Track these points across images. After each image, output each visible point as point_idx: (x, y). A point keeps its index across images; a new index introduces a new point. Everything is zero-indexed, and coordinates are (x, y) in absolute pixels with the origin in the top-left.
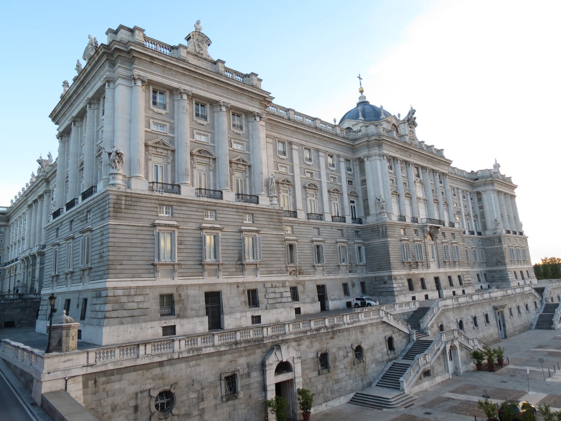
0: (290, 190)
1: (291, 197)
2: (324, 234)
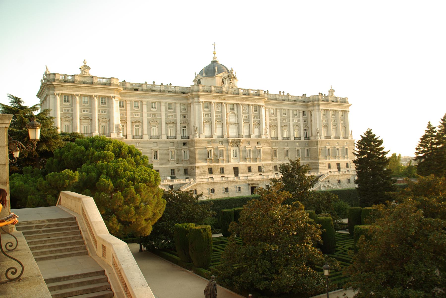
0: (140, 126)
1: (140, 128)
2: (160, 145)
